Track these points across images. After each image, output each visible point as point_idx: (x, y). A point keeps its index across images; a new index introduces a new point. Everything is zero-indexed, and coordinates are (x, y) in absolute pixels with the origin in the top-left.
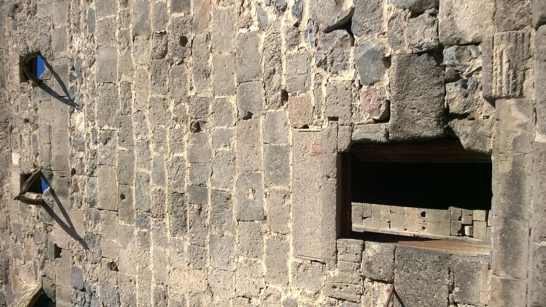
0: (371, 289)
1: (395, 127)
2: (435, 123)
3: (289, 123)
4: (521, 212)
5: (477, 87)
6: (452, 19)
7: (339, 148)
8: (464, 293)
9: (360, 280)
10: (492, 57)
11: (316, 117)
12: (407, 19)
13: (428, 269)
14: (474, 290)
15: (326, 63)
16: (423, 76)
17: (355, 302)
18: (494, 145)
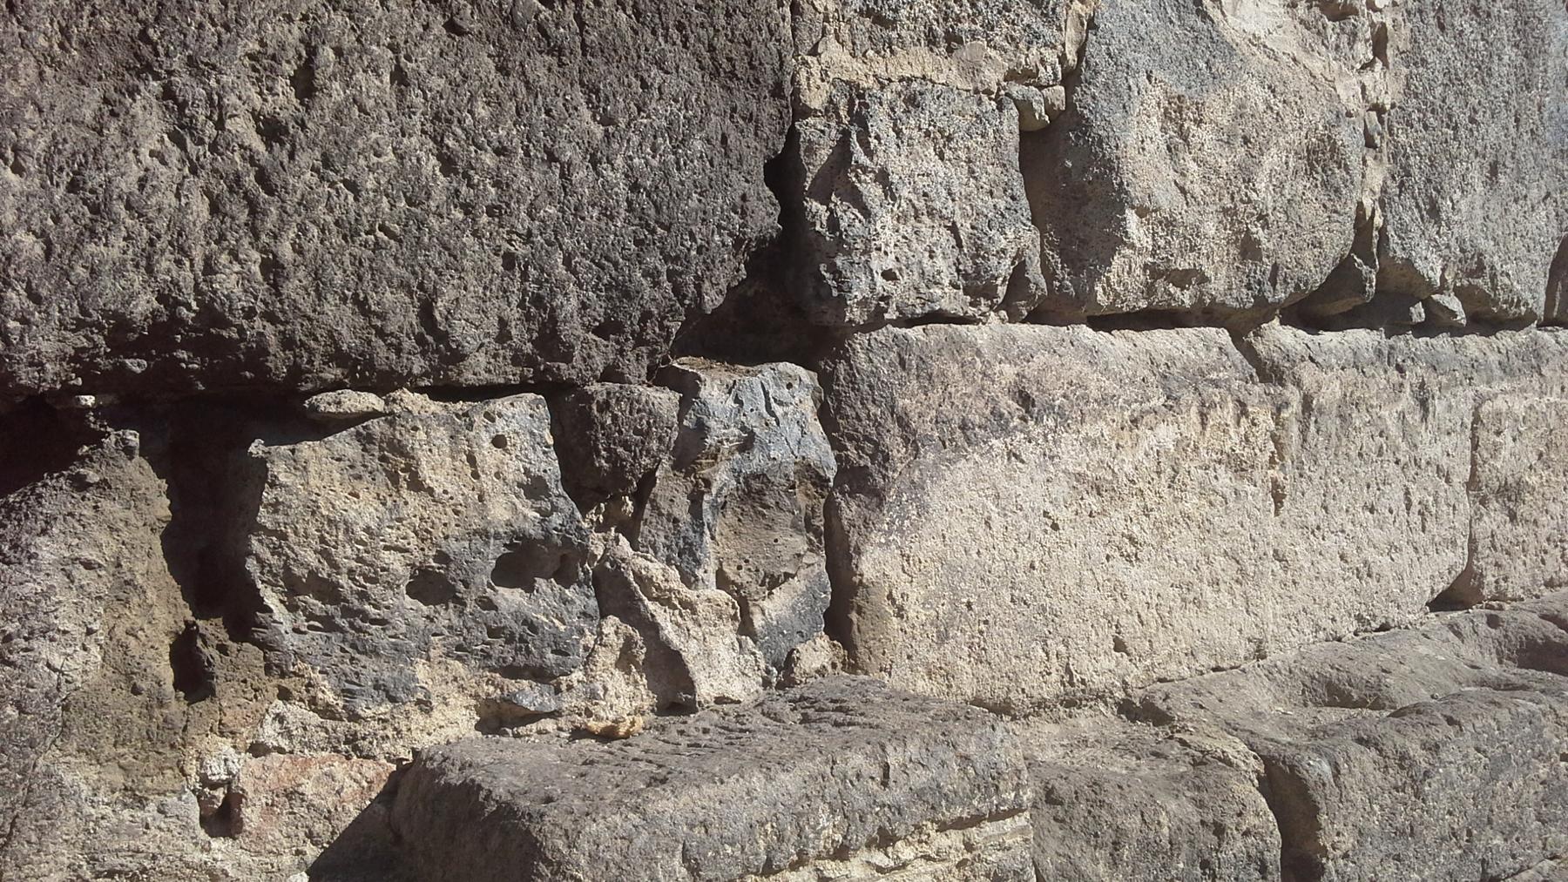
2: (144, 305)
5: (512, 672)
6: (1000, 424)
10: (885, 840)
12: (1017, 89)
16: (622, 188)
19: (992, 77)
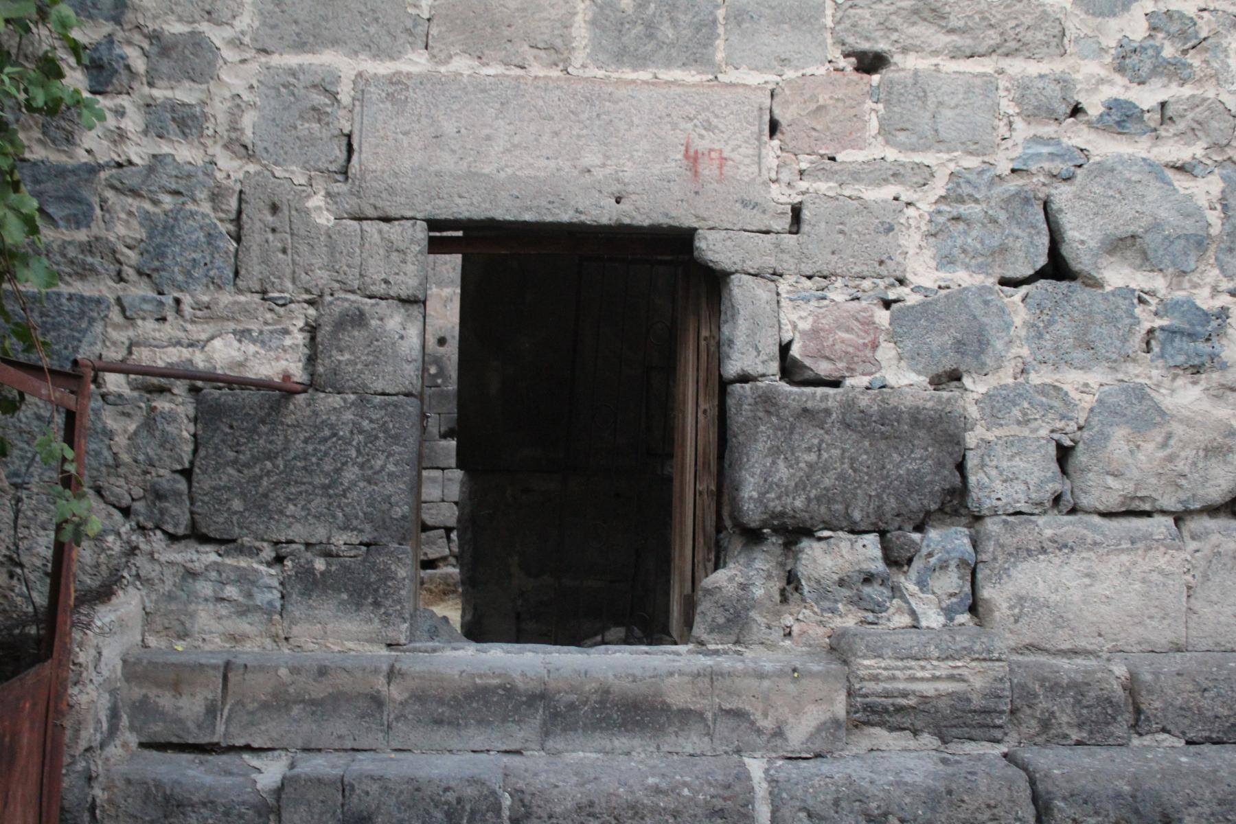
0: (286, 324)
1: (768, 401)
3: (790, 74)
4: (564, 730)
6: (1044, 551)
7: (711, 235)
8: (309, 583)
9: (308, 291)
11: (804, 166)
13: (370, 488)
14: (326, 608)
15: (960, 200)
17: (237, 274)
18: (716, 652)
19: (1044, 432)
